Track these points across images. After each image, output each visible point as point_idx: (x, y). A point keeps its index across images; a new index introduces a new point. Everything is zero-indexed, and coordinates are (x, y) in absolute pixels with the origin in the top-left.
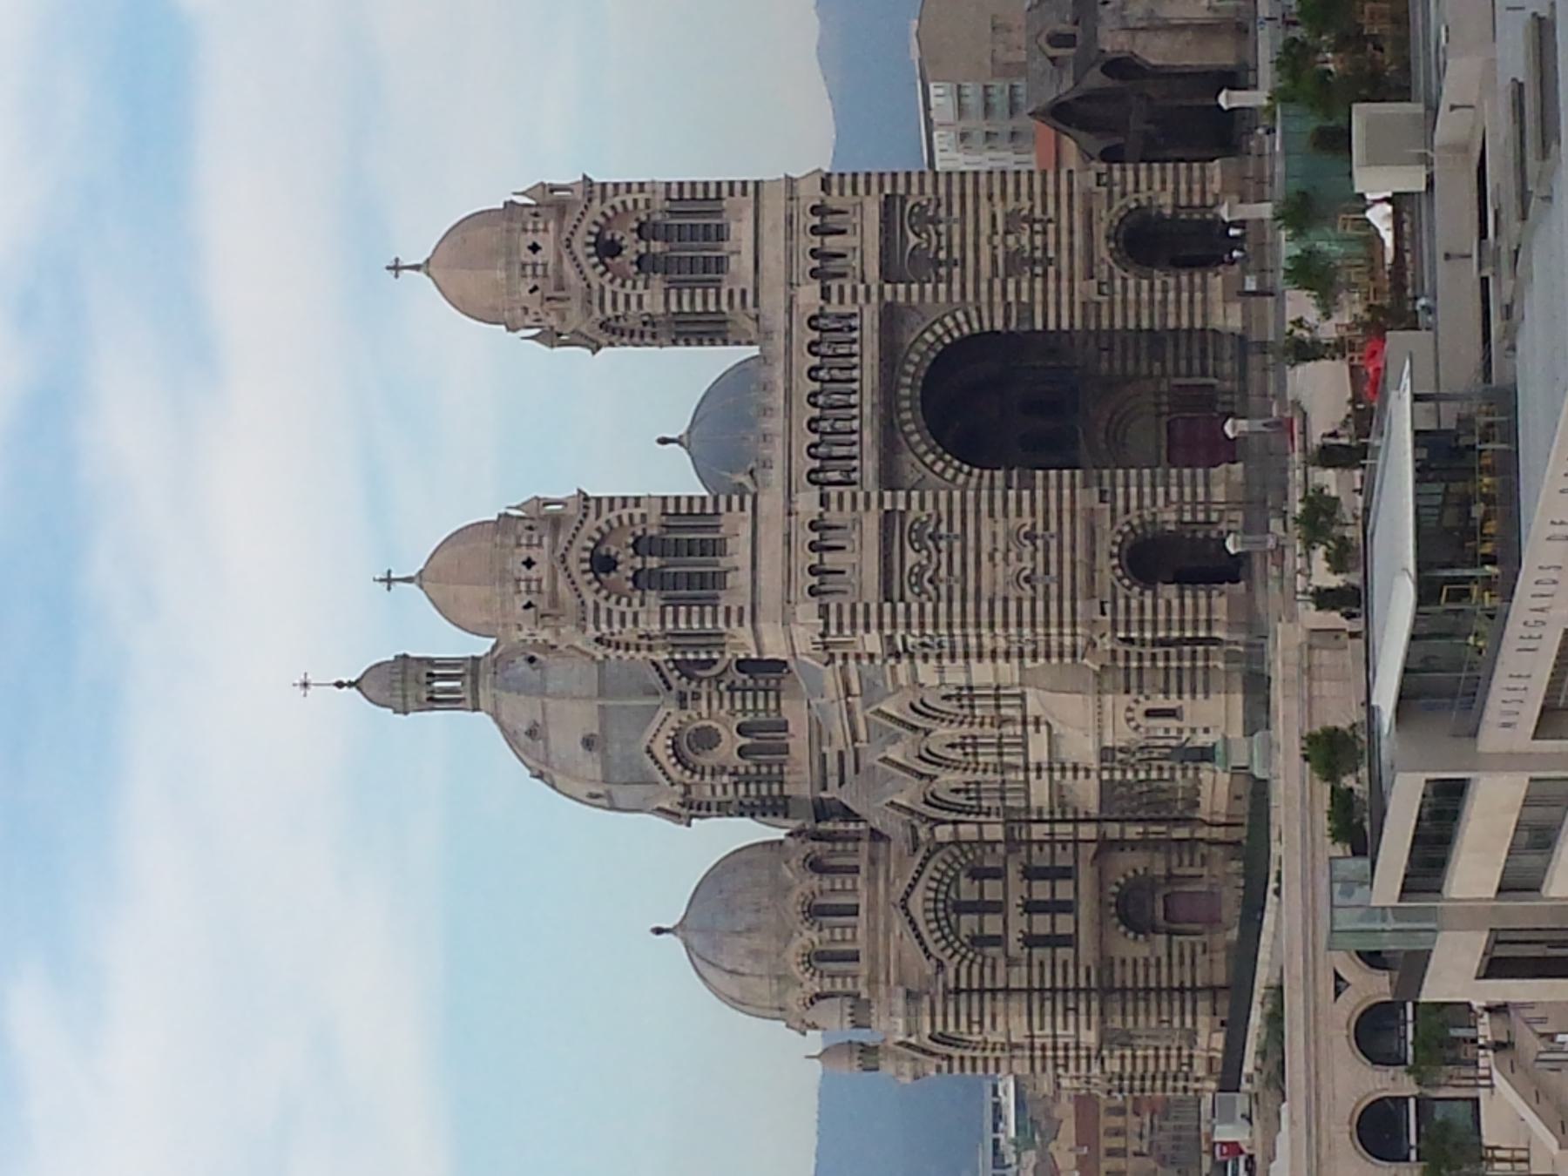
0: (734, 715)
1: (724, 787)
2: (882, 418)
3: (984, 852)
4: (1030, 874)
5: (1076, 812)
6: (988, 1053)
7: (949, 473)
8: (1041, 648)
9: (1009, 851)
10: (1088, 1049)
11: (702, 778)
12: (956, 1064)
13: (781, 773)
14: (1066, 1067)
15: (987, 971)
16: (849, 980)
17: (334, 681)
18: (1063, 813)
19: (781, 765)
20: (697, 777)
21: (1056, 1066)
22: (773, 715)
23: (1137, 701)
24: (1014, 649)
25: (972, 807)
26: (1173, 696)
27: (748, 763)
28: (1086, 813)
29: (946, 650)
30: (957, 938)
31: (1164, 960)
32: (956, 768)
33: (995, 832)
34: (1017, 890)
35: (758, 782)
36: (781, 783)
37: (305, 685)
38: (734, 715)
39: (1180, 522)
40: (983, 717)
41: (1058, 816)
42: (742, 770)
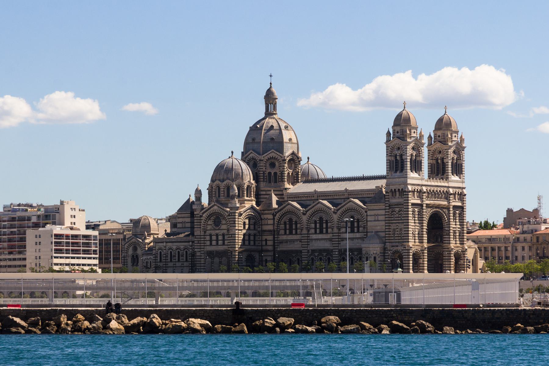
0: (280, 171)
1: (262, 169)
2: (434, 205)
3: (258, 226)
4: (255, 235)
5: (277, 245)
6: (202, 225)
7: (427, 218)
8: (390, 236)
9: (259, 232)
10: (204, 248)
11: (264, 164)
12: (199, 218)
13: (265, 181)
14: (198, 243)
15: (241, 225)
16: (223, 195)
17: (272, 83)
18: (277, 243)
19: (266, 181)
20: (265, 163)
21: (198, 241)
22: (280, 180)
23: (378, 255)
24: (390, 230)
25: (280, 223)
26: (379, 262)
27: (267, 174)
28: (277, 248)
29: (390, 216)
30: (245, 219)
31: (242, 265)
32: (309, 219)
33: (266, 228)
34: (252, 232)
35: (263, 176)
36: (263, 181)
37: (271, 76)
38: (280, 171)
39: (420, 264)
40: (340, 224)
41: (275, 242)
42: (265, 173)
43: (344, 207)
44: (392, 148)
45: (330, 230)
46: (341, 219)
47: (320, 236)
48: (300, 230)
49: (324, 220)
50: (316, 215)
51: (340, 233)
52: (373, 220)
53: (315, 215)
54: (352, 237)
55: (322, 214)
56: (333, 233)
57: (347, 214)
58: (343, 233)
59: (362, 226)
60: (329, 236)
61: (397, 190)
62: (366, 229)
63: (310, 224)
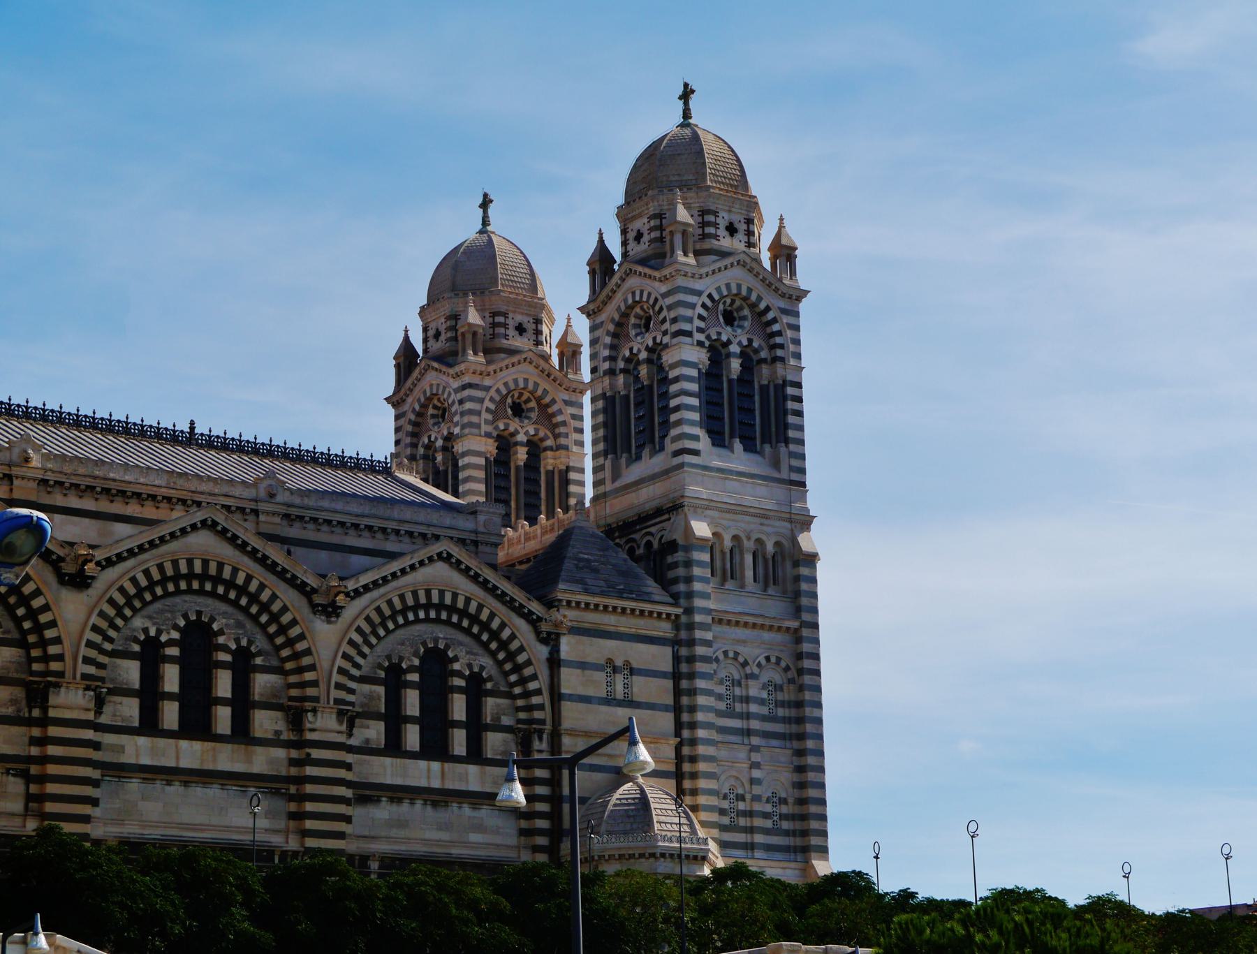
40: (351, 691)
43: (394, 584)
44: (709, 303)
45: (265, 722)
46: (359, 660)
47: (190, 753)
48: (19, 692)
49: (225, 648)
50: (158, 605)
51: (350, 749)
52: (602, 693)
53: (156, 598)
54: (436, 784)
55: (209, 606)
56: (299, 744)
57: (401, 633)
58: (366, 750)
59: (506, 721)
60: (263, 761)
61: (749, 545)
62: (544, 746)
63: (113, 654)
